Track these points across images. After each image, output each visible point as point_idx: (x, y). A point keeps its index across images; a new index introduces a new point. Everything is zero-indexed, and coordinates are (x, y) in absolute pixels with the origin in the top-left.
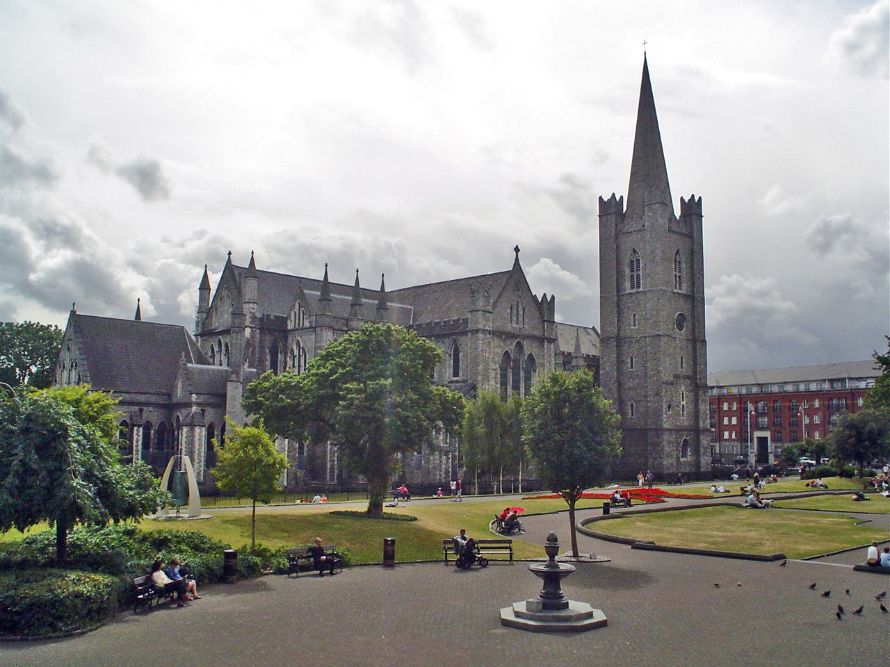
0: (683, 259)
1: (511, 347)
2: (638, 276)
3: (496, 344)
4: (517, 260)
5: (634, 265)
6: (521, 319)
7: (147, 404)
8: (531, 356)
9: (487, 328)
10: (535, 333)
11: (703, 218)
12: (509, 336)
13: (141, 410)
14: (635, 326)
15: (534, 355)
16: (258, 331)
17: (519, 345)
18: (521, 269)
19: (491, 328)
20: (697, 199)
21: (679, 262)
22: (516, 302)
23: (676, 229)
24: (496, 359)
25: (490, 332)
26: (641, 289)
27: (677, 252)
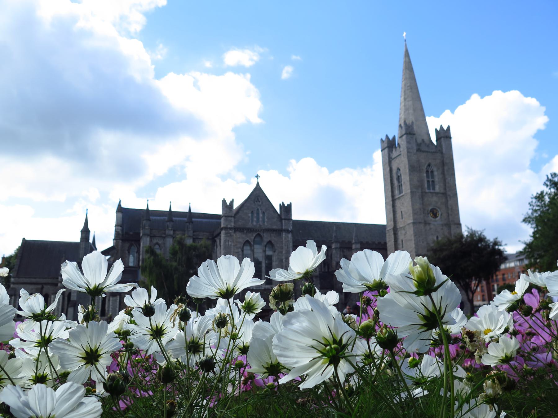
0: (435, 169)
1: (251, 237)
2: (402, 184)
3: (238, 236)
4: (258, 184)
5: (399, 178)
6: (260, 219)
7: (46, 284)
8: (270, 242)
9: (229, 226)
10: (274, 227)
11: (453, 140)
12: (250, 230)
13: (42, 288)
14: (402, 218)
15: (273, 242)
16: (120, 241)
17: (259, 235)
18: (261, 189)
19: (233, 226)
20: (445, 128)
21: (432, 172)
22: (257, 209)
23: (426, 149)
24: (239, 245)
25: (231, 229)
26: (403, 194)
27: (429, 165)
